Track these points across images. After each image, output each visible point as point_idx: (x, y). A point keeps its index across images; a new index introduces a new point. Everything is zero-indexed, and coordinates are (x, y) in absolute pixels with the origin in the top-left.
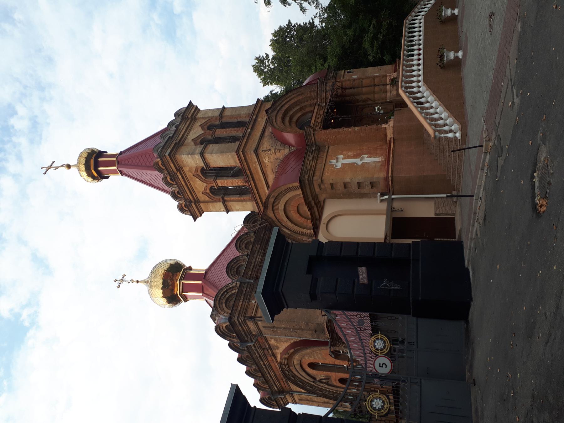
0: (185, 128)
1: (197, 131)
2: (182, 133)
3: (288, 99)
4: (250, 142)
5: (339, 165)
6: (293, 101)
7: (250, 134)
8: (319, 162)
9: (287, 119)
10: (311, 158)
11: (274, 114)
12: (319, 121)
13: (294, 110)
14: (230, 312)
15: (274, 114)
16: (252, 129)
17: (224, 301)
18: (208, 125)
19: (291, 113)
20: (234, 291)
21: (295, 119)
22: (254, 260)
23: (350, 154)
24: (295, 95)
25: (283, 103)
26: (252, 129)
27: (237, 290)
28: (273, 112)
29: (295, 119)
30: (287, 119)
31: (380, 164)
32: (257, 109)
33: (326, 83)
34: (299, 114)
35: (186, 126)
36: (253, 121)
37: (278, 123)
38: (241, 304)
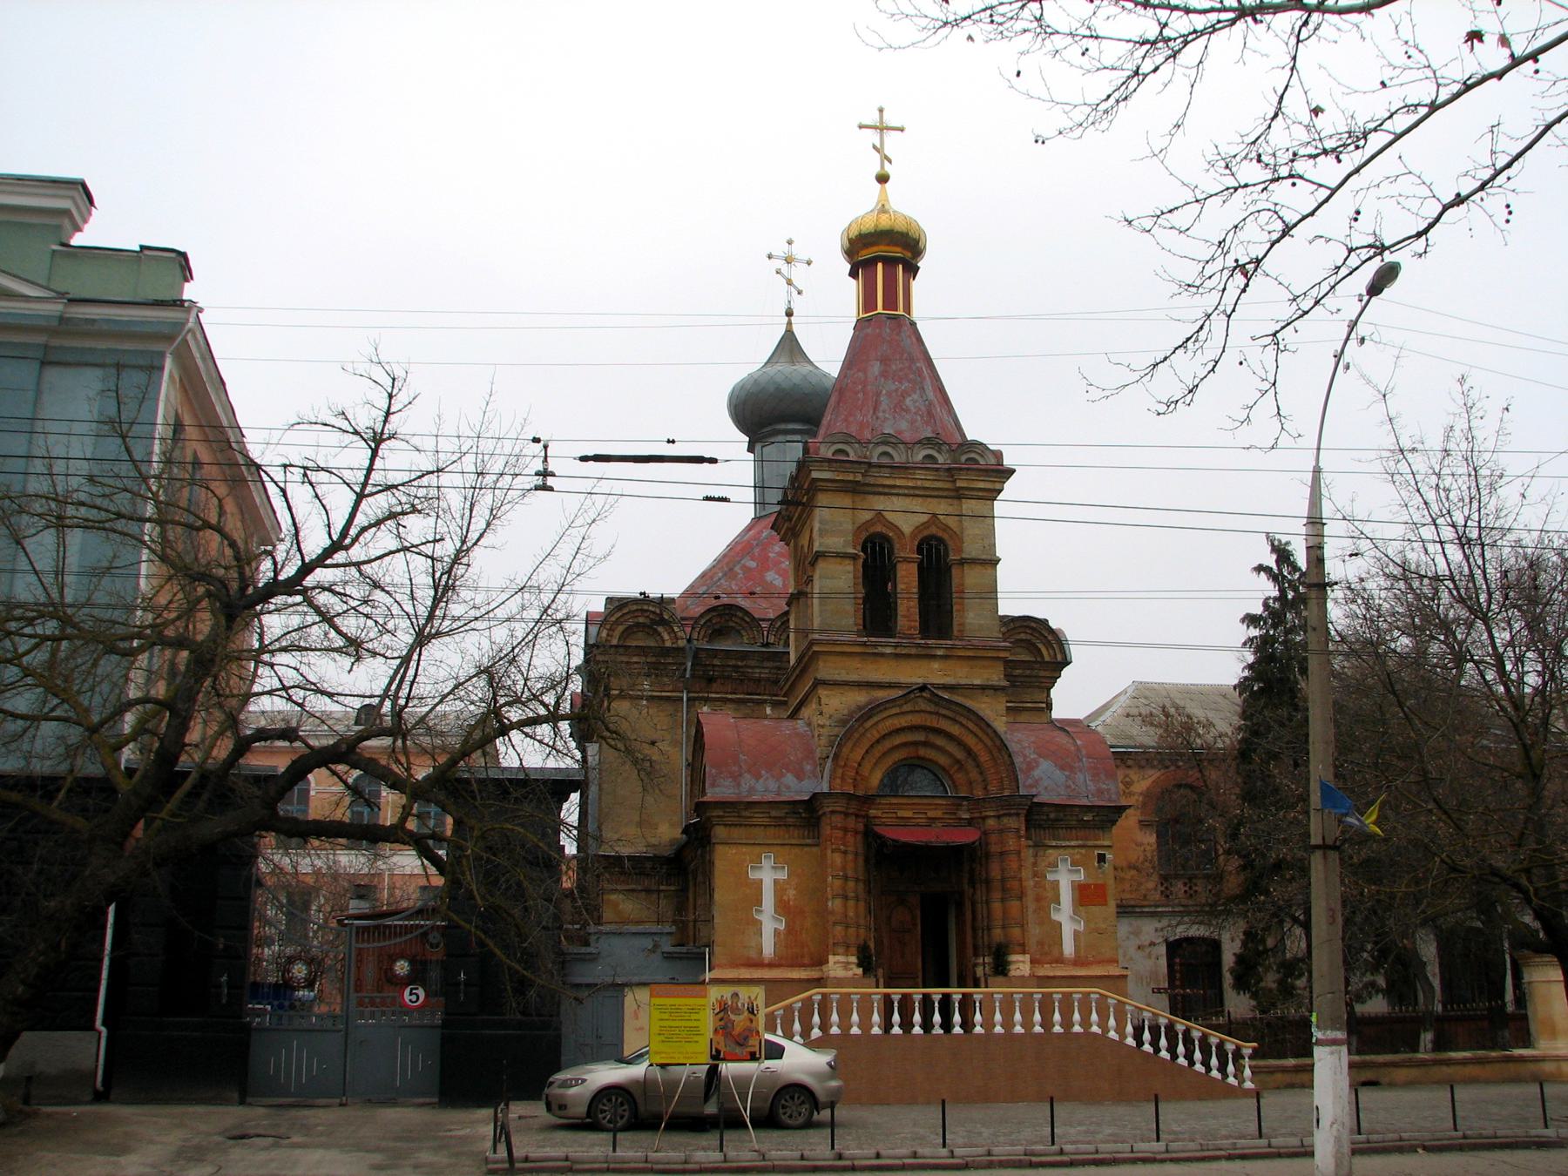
0: (919, 483)
1: (906, 516)
2: (898, 482)
3: (975, 729)
4: (855, 663)
5: (753, 875)
6: (971, 741)
7: (883, 655)
8: (771, 831)
9: (920, 737)
10: (774, 813)
11: (923, 705)
12: (901, 813)
13: (951, 748)
14: (615, 642)
15: (923, 705)
16: (897, 656)
17: (641, 620)
18: (940, 534)
19: (940, 741)
20: (666, 637)
21: (922, 752)
22: (752, 663)
23: (792, 893)
24: (989, 743)
25: (961, 719)
26: (897, 656)
27: (668, 644)
28: (930, 700)
29: (922, 752)
30: (920, 737)
31: (753, 954)
32: (970, 654)
33: (1018, 815)
34: (943, 760)
35: (927, 484)
36: (924, 652)
37: (889, 723)
38: (635, 659)
